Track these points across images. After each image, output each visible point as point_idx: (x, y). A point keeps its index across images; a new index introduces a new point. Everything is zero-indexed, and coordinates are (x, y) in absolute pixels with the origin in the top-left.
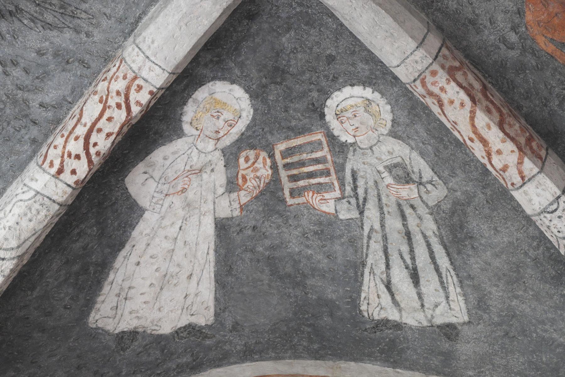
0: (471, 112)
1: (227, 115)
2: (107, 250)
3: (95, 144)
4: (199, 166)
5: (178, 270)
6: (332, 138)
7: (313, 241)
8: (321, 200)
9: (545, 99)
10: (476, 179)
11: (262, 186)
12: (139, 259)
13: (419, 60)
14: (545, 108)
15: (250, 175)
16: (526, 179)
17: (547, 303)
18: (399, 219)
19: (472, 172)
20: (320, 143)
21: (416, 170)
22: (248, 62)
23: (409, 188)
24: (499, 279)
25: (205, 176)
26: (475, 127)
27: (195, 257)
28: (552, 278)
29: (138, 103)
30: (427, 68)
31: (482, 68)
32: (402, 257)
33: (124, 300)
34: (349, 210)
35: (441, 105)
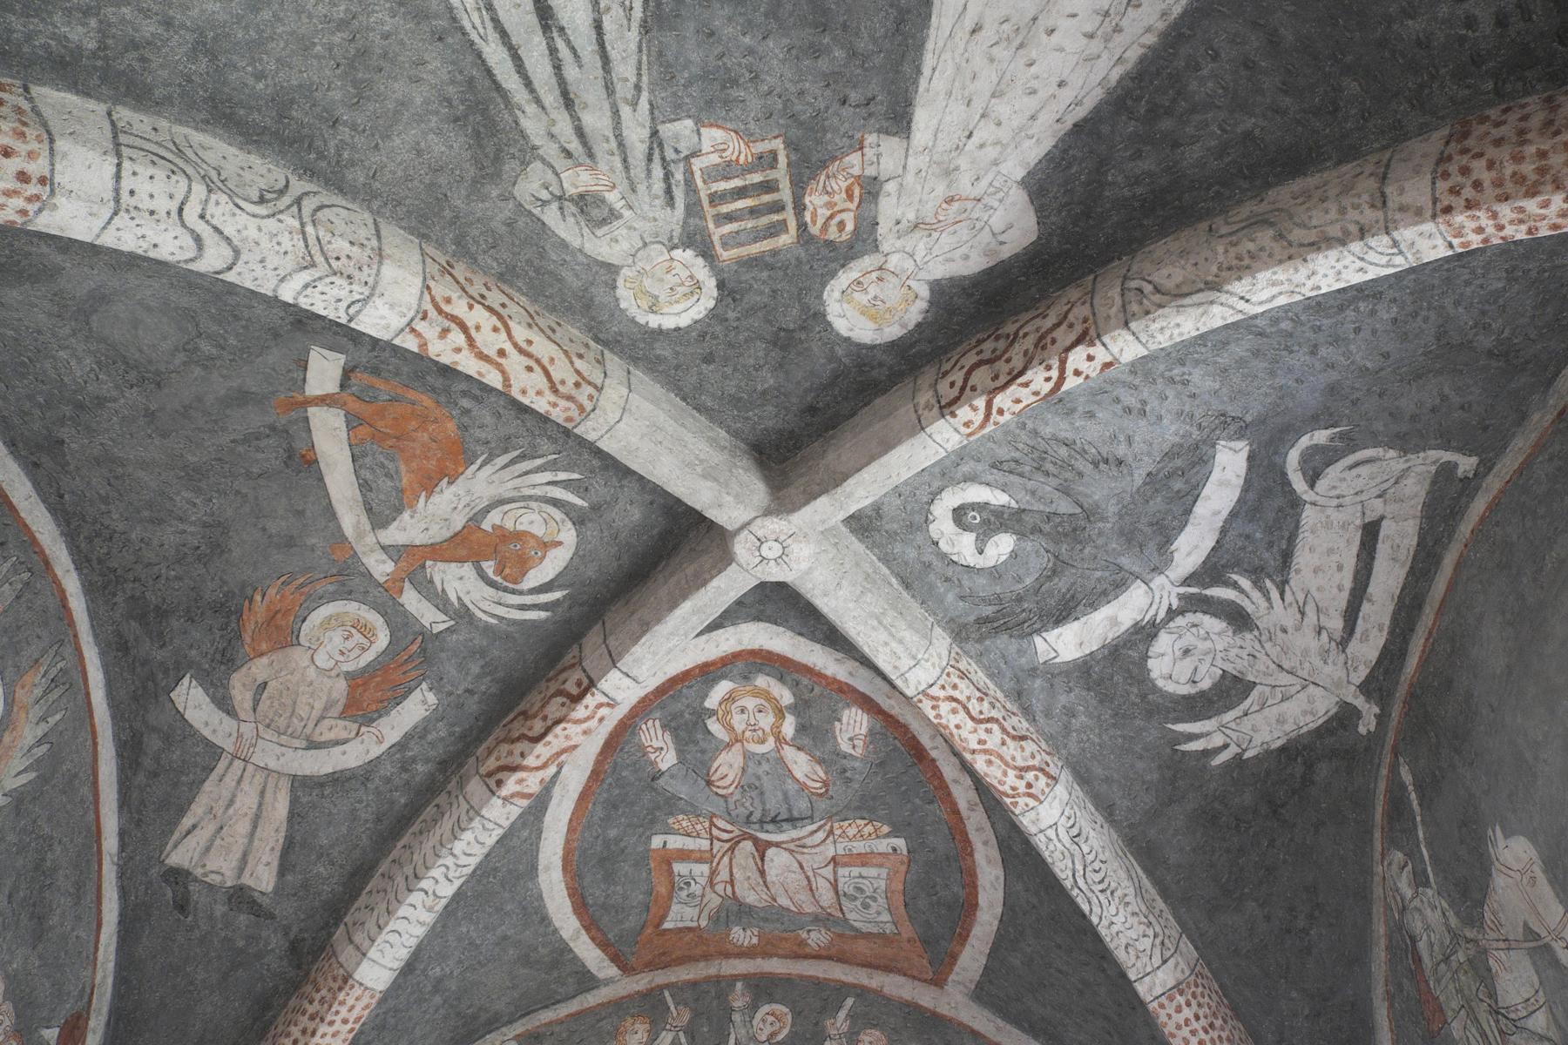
1: (862, 298)
2: (1105, 129)
3: (1048, 379)
4: (917, 234)
5: (995, 51)
6: (707, 253)
7: (740, 65)
8: (724, 150)
10: (472, 224)
11: (823, 178)
12: (1058, 92)
15: (839, 198)
16: (407, 330)
17: (282, 44)
18: (587, 130)
19: (481, 234)
20: (725, 245)
21: (571, 220)
22: (822, 361)
23: (577, 187)
24: (385, 56)
25: (911, 216)
27: (958, 68)
28: (292, 101)
29: (975, 409)
32: (574, 50)
33: (1111, 12)
34: (677, 137)
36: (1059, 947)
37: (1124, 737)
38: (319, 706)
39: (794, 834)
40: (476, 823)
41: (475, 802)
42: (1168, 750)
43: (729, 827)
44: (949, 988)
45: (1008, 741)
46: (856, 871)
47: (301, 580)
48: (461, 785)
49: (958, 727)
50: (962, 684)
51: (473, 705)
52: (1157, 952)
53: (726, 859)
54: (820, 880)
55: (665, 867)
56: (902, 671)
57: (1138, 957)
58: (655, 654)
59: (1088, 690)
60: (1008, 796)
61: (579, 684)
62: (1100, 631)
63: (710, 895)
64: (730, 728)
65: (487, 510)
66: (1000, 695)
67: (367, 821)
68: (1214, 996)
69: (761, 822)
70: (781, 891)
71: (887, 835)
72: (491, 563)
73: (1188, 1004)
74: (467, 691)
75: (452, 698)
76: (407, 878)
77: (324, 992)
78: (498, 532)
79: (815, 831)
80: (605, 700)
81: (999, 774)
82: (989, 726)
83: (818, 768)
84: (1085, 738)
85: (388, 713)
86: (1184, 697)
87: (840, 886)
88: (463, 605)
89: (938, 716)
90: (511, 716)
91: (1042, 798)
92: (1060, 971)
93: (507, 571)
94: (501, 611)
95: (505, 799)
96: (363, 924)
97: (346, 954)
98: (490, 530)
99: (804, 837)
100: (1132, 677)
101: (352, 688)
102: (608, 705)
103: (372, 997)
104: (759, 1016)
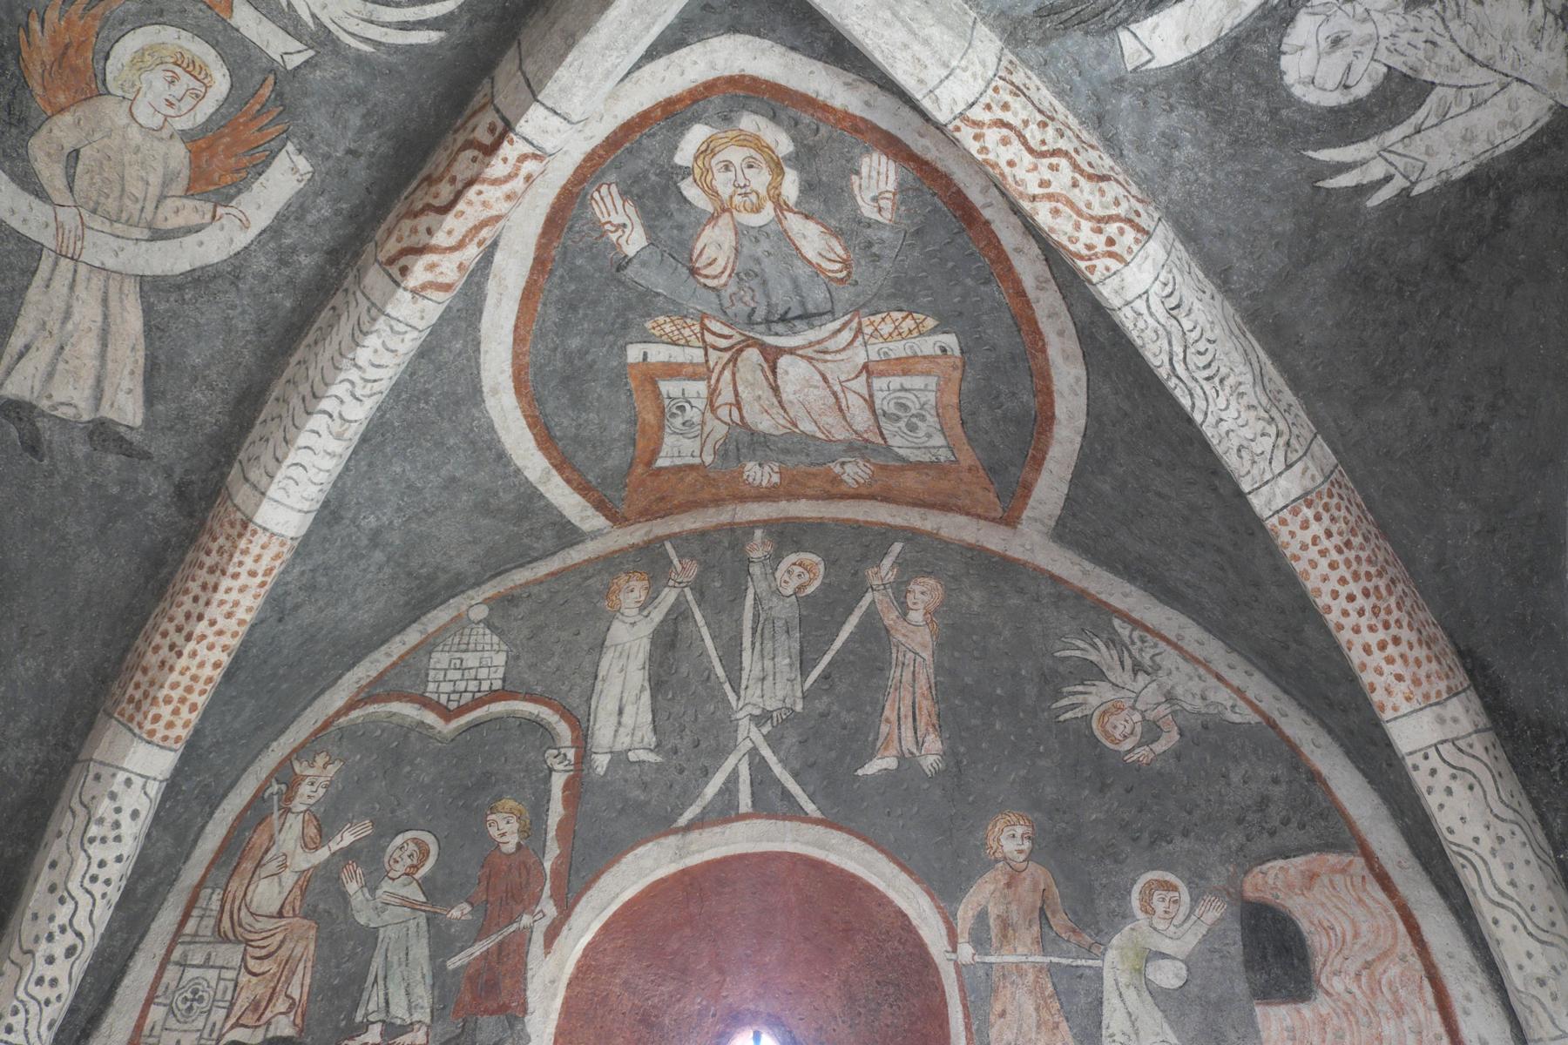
36: (1158, 464)
37: (1247, 174)
38: (155, 180)
39: (812, 335)
40: (381, 323)
41: (376, 297)
42: (1307, 189)
43: (726, 331)
44: (1024, 527)
45: (1082, 181)
46: (896, 382)
48: (358, 280)
49: (1011, 164)
50: (1017, 103)
51: (360, 172)
52: (1280, 455)
53: (727, 374)
54: (851, 396)
55: (649, 387)
56: (931, 85)
57: (1254, 462)
58: (588, 79)
59: (1197, 106)
60: (1082, 258)
61: (492, 129)
62: (1213, 16)
63: (711, 423)
64: (713, 193)
66: (1072, 121)
67: (246, 332)
68: (1354, 509)
69: (768, 321)
70: (802, 413)
71: (933, 331)
73: (1318, 518)
74: (349, 152)
75: (330, 163)
76: (304, 399)
77: (221, 541)
79: (839, 331)
80: (528, 149)
81: (1069, 228)
82: (1054, 160)
83: (834, 243)
84: (1192, 178)
85: (249, 187)
86: (1331, 110)
87: (878, 402)
89: (984, 150)
90: (414, 184)
91: (1128, 258)
92: (1159, 494)
94: (374, 33)
95: (414, 292)
96: (258, 458)
97: (242, 495)
99: (823, 340)
100: (1257, 84)
101: (195, 155)
102: (535, 156)
103: (283, 544)
104: (783, 566)
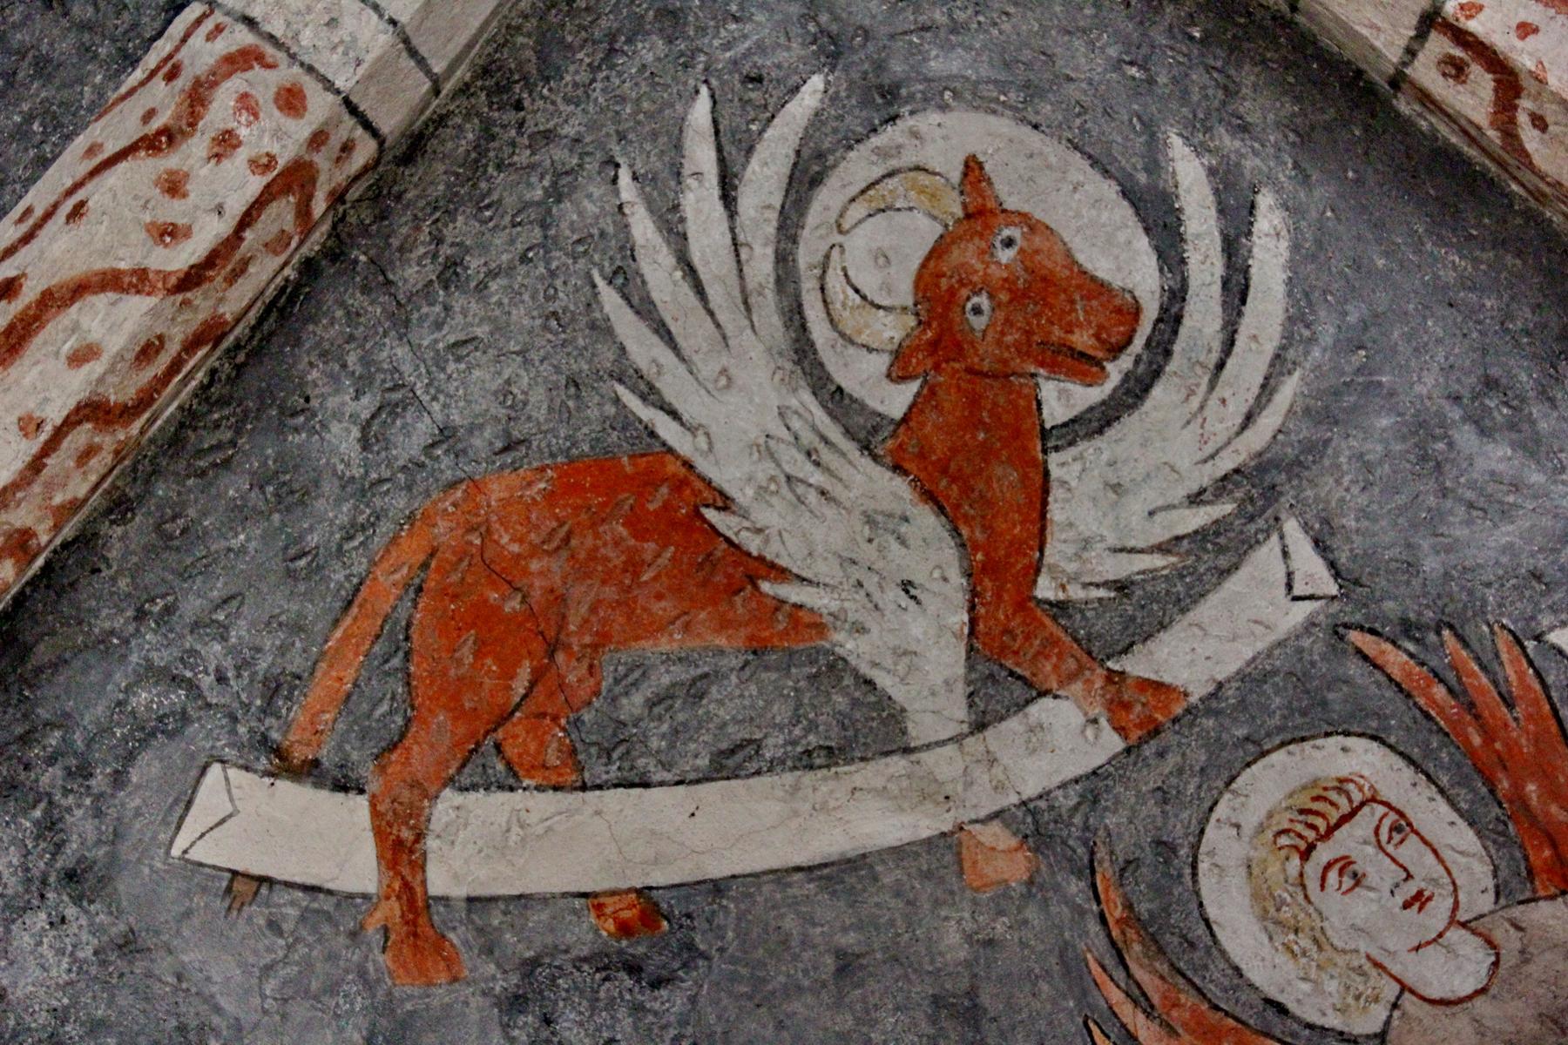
0: (142, 274)
9: (168, 610)
13: (342, 33)
14: (130, 613)
26: (73, 300)
30: (310, 69)
31: (272, 334)
35: (152, 143)
47: (1116, 996)
65: (836, 399)
72: (1049, 391)
78: (916, 361)
88: (1224, 484)
93: (1082, 339)
94: (1249, 366)
98: (913, 387)
